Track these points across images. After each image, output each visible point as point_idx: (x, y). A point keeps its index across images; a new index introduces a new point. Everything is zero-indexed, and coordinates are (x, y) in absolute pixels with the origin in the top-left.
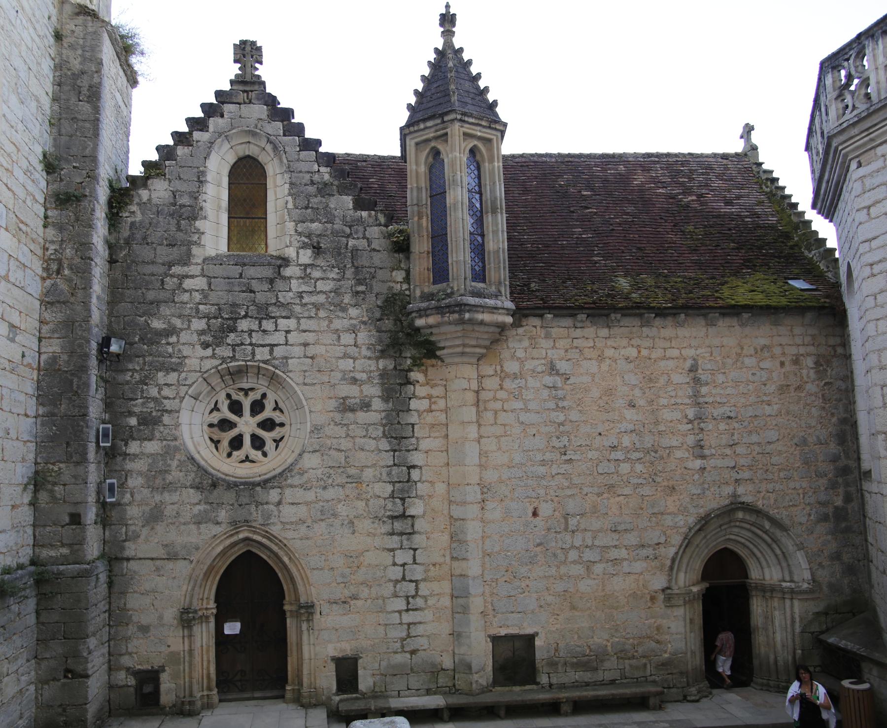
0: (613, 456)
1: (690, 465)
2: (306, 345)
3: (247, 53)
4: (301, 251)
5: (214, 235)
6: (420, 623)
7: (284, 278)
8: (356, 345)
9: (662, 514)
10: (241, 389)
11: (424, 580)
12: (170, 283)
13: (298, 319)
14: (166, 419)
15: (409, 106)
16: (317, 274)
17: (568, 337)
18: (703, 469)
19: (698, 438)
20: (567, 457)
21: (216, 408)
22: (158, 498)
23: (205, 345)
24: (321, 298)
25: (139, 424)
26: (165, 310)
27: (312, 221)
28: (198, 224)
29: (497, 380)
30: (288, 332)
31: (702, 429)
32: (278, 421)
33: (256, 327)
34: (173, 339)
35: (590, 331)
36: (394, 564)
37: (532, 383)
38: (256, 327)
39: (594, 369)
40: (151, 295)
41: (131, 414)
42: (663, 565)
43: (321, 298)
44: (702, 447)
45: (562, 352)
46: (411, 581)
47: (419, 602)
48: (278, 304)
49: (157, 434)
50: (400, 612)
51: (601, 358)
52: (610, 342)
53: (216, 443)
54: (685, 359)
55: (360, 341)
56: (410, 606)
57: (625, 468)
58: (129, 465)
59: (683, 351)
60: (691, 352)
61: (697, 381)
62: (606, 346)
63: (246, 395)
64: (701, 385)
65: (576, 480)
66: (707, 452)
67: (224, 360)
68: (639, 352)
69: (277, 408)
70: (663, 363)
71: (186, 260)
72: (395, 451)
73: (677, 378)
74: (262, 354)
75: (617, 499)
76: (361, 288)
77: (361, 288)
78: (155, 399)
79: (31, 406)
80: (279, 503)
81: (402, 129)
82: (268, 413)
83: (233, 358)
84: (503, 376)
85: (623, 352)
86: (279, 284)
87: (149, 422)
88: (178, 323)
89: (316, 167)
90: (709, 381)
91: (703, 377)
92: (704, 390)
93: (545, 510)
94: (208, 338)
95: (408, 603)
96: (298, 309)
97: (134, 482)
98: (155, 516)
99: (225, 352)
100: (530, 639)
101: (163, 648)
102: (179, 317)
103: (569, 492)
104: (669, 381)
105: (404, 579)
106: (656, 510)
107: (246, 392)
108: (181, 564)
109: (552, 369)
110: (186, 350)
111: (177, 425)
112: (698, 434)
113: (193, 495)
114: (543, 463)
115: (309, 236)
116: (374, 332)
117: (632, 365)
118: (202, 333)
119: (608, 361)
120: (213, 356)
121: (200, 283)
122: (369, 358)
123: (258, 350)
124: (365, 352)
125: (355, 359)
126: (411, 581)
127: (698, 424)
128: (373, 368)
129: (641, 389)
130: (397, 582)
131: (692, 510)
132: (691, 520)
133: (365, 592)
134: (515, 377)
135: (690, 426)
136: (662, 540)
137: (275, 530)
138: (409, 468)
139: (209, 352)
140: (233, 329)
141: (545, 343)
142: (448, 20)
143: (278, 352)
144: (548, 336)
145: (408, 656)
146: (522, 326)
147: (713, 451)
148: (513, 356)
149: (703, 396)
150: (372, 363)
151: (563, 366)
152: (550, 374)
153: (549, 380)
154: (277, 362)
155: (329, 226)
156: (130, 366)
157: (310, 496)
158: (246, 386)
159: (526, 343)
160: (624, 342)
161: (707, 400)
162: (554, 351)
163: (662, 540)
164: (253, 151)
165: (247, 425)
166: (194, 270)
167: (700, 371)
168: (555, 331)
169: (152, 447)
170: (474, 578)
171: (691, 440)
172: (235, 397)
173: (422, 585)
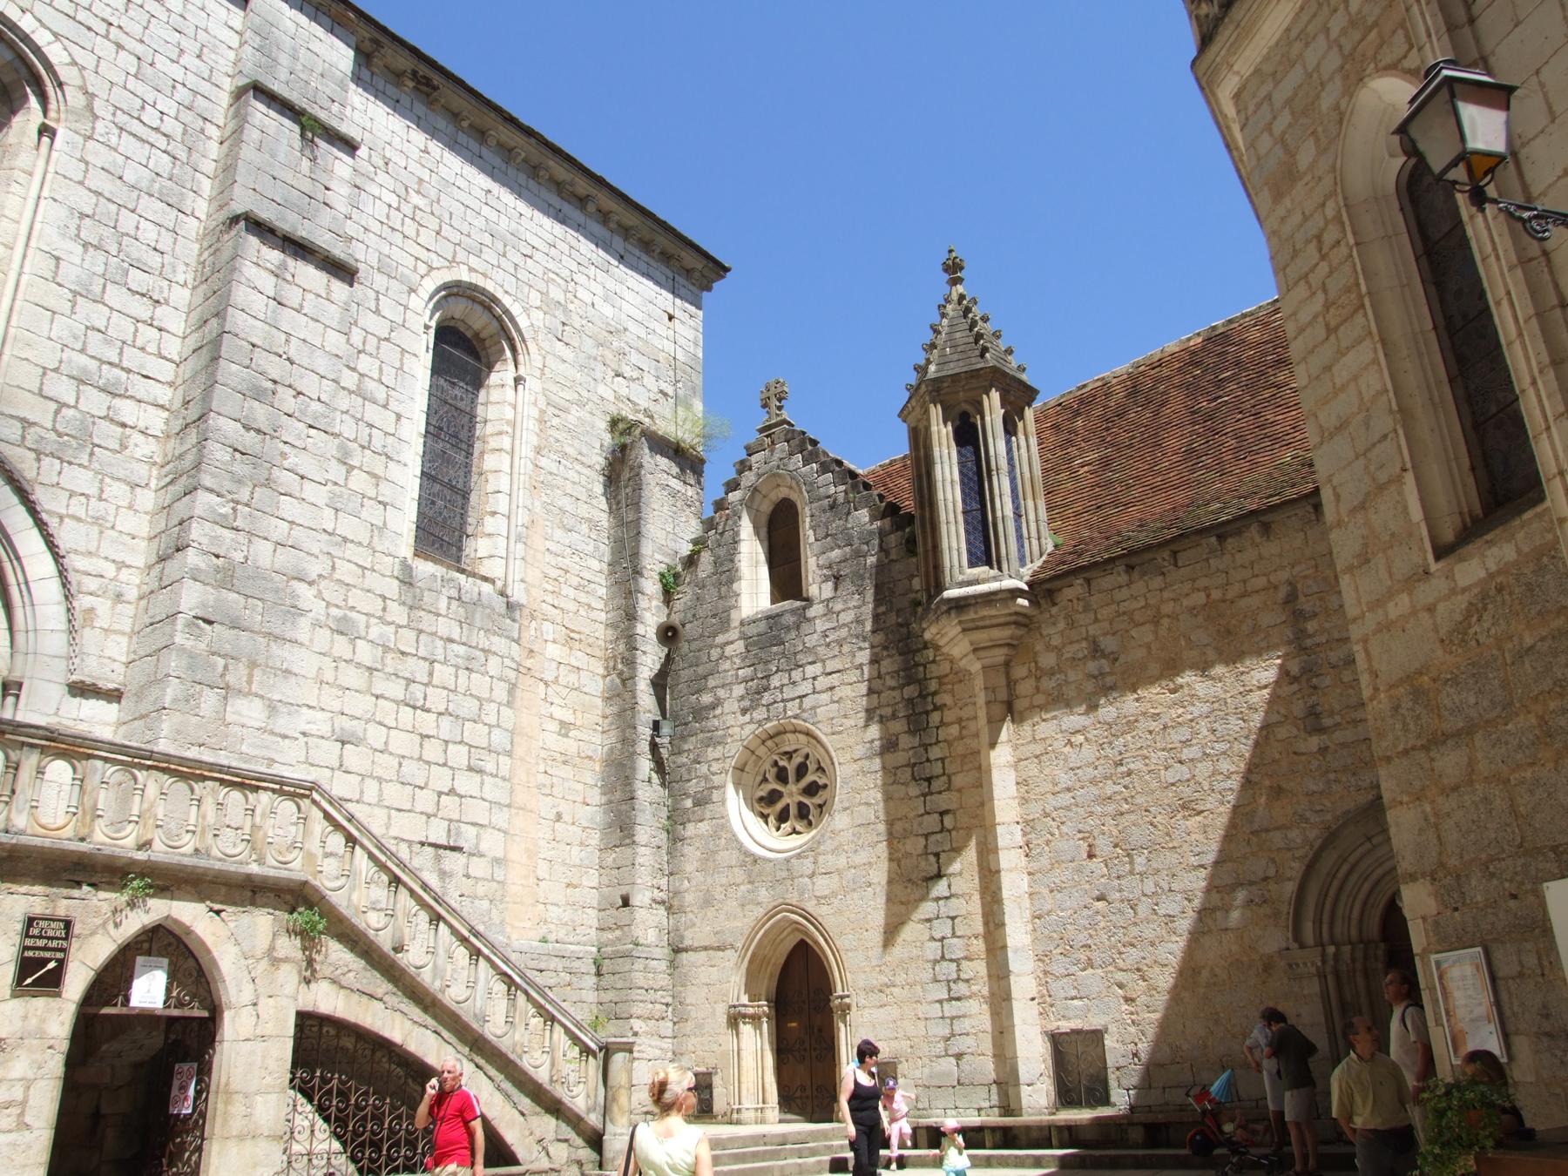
0: (1187, 754)
1: (1302, 747)
2: (832, 688)
3: (774, 397)
4: (824, 586)
5: (754, 591)
6: (964, 1016)
7: (809, 620)
8: (879, 677)
9: (1267, 830)
10: (786, 753)
11: (966, 958)
12: (715, 653)
13: (823, 661)
14: (715, 796)
15: (909, 388)
16: (838, 607)
17: (1113, 601)
18: (1323, 750)
19: (1310, 703)
20: (1124, 769)
21: (765, 780)
22: (709, 880)
23: (744, 711)
24: (844, 632)
25: (695, 805)
26: (711, 683)
27: (832, 549)
28: (735, 586)
29: (1032, 681)
30: (814, 678)
31: (1315, 688)
32: (821, 782)
33: (786, 681)
34: (718, 711)
35: (1139, 587)
36: (933, 939)
37: (1072, 676)
38: (786, 681)
39: (1150, 638)
40: (701, 670)
41: (687, 795)
42: (1276, 914)
43: (844, 632)
44: (1317, 715)
45: (1106, 625)
46: (951, 960)
47: (961, 989)
48: (808, 650)
49: (708, 815)
50: (940, 1002)
51: (1156, 621)
52: (1166, 595)
53: (765, 817)
54: (1276, 588)
55: (883, 671)
56: (953, 994)
57: (1203, 769)
58: (687, 849)
59: (1272, 578)
60: (1284, 575)
61: (1298, 616)
62: (1162, 601)
63: (790, 758)
64: (1306, 619)
65: (1140, 800)
66: (1327, 722)
67: (760, 723)
68: (1208, 596)
69: (820, 769)
70: (1244, 602)
71: (725, 625)
72: (924, 795)
73: (1266, 619)
74: (792, 709)
75: (1199, 818)
76: (883, 609)
77: (883, 609)
78: (706, 778)
79: (596, 797)
80: (811, 876)
81: (903, 414)
82: (810, 777)
83: (768, 719)
84: (1039, 674)
85: (1185, 602)
86: (805, 627)
87: (701, 802)
88: (721, 693)
89: (832, 490)
90: (1317, 610)
91: (1307, 607)
92: (1311, 626)
93: (1103, 846)
94: (746, 703)
95: (950, 990)
96: (821, 650)
97: (690, 867)
98: (707, 901)
99: (760, 714)
100: (1097, 1036)
101: (715, 1047)
102: (723, 686)
103: (1133, 817)
104: (1255, 630)
105: (943, 957)
106: (1256, 827)
107: (789, 755)
108: (729, 953)
109: (1096, 651)
110: (730, 720)
111: (723, 802)
112: (1310, 696)
113: (739, 875)
114: (1093, 782)
115: (830, 567)
116: (898, 658)
117: (1200, 619)
118: (742, 698)
119: (1165, 622)
120: (751, 722)
121: (739, 646)
122: (893, 689)
123: (789, 705)
124: (890, 682)
125: (879, 693)
126: (951, 960)
127: (1308, 680)
128: (898, 699)
129: (1216, 648)
130: (936, 962)
131: (1314, 818)
132: (1313, 834)
133: (901, 978)
134: (1052, 673)
135: (1295, 687)
136: (1271, 872)
137: (810, 906)
138: (942, 814)
139: (748, 717)
140: (766, 689)
141: (1083, 619)
142: (953, 269)
143: (807, 702)
144: (1087, 609)
145: (953, 1060)
146: (1054, 604)
147: (1338, 718)
148: (1049, 647)
149: (1310, 636)
150: (896, 693)
151: (1109, 644)
152: (1094, 658)
153: (1092, 666)
154: (805, 715)
155: (847, 549)
156: (686, 747)
157: (842, 861)
158: (788, 749)
159: (1062, 625)
160: (1187, 587)
161: (1317, 639)
162: (1096, 626)
163: (1271, 872)
164: (783, 492)
165: (792, 794)
166: (733, 634)
167: (1302, 599)
168: (1095, 600)
169: (704, 827)
170: (1016, 951)
171: (1298, 708)
172: (781, 763)
173: (964, 964)
